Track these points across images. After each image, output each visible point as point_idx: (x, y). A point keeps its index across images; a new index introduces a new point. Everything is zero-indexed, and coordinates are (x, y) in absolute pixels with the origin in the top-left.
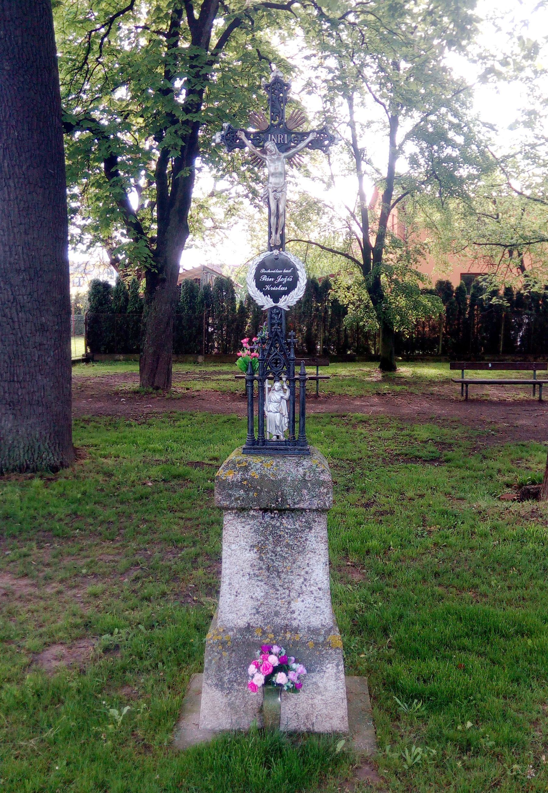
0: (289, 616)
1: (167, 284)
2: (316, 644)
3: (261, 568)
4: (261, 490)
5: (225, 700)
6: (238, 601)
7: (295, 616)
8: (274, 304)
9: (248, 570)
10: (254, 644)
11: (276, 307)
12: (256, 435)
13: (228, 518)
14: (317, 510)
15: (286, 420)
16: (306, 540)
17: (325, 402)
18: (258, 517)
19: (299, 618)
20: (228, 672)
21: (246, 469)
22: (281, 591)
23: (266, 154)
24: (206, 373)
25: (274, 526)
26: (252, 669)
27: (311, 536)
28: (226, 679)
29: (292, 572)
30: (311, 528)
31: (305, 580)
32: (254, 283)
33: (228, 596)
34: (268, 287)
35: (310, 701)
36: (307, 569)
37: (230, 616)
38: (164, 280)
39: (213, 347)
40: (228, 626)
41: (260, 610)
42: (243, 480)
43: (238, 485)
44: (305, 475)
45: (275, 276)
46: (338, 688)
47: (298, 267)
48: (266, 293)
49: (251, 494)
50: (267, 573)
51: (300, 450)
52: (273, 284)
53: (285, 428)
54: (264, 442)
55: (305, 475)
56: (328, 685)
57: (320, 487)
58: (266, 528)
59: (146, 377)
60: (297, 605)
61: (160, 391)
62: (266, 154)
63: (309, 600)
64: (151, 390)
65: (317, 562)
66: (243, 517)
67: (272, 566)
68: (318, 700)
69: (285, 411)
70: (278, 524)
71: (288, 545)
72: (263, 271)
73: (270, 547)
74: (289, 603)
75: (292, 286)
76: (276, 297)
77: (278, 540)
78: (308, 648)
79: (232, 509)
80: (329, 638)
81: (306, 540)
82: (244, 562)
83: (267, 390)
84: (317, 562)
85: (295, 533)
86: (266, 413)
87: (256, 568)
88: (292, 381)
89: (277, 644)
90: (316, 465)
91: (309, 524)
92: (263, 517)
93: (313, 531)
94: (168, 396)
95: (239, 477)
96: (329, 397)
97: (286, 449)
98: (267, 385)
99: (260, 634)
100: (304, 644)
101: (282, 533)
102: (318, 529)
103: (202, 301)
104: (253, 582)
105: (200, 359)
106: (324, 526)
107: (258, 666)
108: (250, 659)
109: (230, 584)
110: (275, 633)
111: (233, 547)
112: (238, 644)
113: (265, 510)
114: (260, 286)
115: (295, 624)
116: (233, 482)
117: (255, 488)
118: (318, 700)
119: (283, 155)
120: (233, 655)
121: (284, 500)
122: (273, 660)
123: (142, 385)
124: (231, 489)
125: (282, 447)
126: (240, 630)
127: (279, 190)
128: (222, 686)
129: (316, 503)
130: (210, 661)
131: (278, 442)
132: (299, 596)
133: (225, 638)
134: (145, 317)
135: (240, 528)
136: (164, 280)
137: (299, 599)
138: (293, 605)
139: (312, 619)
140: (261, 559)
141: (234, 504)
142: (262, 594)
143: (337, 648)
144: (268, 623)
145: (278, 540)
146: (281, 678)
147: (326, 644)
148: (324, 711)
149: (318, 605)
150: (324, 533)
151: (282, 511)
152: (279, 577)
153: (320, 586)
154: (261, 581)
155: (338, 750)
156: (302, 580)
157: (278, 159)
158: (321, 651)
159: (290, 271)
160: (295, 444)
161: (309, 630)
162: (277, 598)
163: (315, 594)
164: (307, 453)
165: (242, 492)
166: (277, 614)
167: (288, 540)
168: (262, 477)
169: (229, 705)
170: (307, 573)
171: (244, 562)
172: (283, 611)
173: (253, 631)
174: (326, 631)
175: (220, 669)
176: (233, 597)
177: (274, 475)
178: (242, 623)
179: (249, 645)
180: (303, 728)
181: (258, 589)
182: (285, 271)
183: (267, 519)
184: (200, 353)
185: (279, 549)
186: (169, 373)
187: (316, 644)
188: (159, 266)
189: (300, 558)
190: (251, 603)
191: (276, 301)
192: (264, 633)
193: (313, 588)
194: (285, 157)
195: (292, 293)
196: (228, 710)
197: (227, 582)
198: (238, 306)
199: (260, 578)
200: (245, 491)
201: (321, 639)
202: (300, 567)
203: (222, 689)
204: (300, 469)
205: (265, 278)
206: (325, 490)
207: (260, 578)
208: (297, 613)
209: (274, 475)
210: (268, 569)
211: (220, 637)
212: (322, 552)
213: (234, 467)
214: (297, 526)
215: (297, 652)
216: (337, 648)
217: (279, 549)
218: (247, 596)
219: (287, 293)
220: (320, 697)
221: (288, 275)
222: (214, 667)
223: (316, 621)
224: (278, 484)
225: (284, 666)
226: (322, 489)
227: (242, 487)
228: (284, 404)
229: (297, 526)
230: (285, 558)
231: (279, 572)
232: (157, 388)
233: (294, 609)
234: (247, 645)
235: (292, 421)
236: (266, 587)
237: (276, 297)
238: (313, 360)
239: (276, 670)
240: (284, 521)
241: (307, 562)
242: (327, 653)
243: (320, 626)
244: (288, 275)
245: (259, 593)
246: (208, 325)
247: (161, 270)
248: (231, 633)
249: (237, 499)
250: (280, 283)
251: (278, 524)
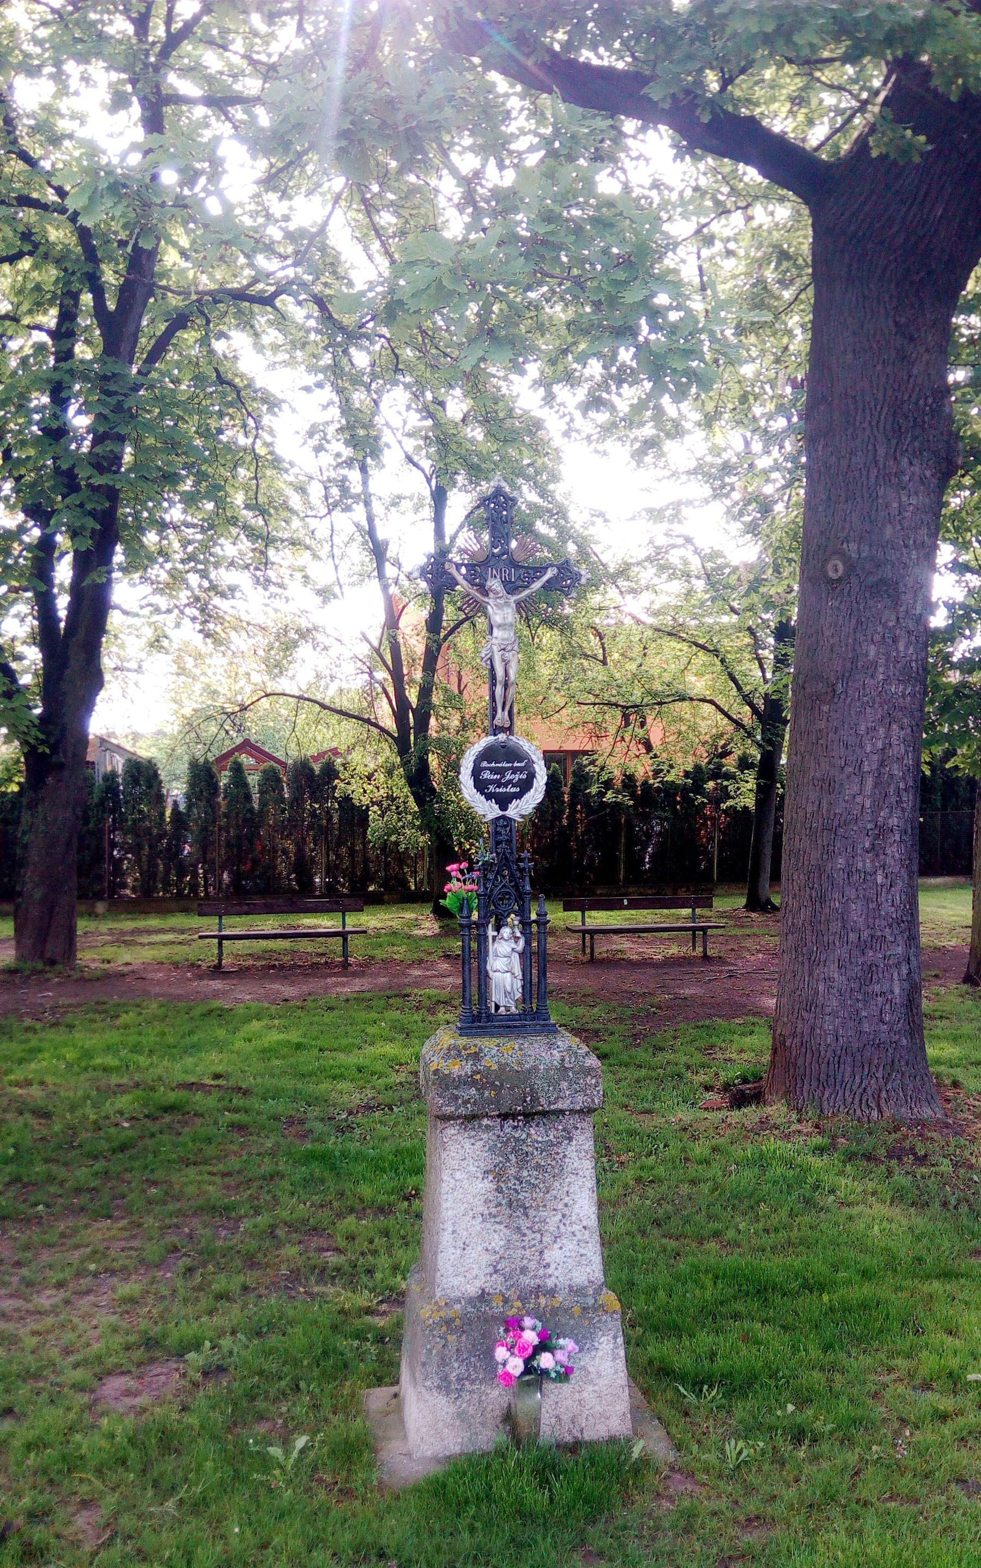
0: (541, 1272)
3: (500, 1204)
7: (550, 1271)
9: (481, 1209)
11: (503, 817)
14: (581, 1111)
15: (520, 984)
17: (362, 974)
21: (476, 1057)
24: (123, 933)
25: (517, 1140)
28: (453, 1377)
30: (570, 1139)
33: (452, 1250)
34: (492, 788)
36: (567, 1200)
37: (455, 1282)
38: (61, 767)
39: (124, 885)
43: (468, 1081)
45: (501, 771)
47: (534, 758)
48: (489, 797)
49: (487, 1094)
50: (508, 1211)
52: (499, 784)
53: (518, 995)
54: (489, 1017)
58: (506, 1144)
60: (554, 1255)
61: (59, 967)
63: (570, 1246)
64: (40, 966)
67: (515, 1199)
68: (588, 1393)
69: (518, 971)
71: (538, 1167)
72: (485, 764)
74: (541, 1253)
75: (526, 785)
76: (503, 802)
78: (572, 1317)
79: (459, 1117)
89: (528, 1314)
94: (76, 975)
95: (468, 1068)
96: (365, 967)
103: (102, 802)
107: (510, 1349)
109: (454, 1232)
111: (458, 1175)
113: (504, 1117)
115: (550, 1283)
118: (588, 1393)
121: (535, 1099)
122: (531, 1337)
125: (517, 1023)
126: (471, 1301)
129: (580, 1101)
131: (511, 1017)
133: (451, 1314)
134: (24, 833)
135: (467, 1145)
136: (61, 767)
139: (575, 1274)
141: (462, 1111)
146: (546, 1361)
147: (600, 1308)
148: (598, 1408)
149: (583, 1251)
150: (589, 1145)
151: (529, 1116)
152: (527, 1215)
160: (531, 1017)
161: (571, 1291)
163: (579, 1236)
165: (473, 1091)
166: (524, 1270)
168: (502, 1067)
172: (533, 1265)
176: (459, 1252)
178: (472, 1290)
179: (486, 1320)
185: (525, 1173)
186: (72, 931)
191: (504, 807)
192: (506, 1301)
193: (575, 1228)
201: (591, 1301)
203: (448, 1392)
205: (487, 775)
208: (553, 1266)
209: (519, 1064)
211: (442, 1314)
212: (587, 1173)
213: (459, 1055)
217: (525, 1173)
219: (519, 796)
220: (591, 1388)
221: (521, 770)
225: (544, 1345)
227: (474, 1083)
228: (516, 958)
230: (535, 1186)
233: (548, 1260)
235: (527, 984)
236: (508, 1232)
237: (503, 802)
244: (521, 770)
245: (497, 1242)
246: (113, 845)
247: (55, 748)
248: (457, 1307)
249: (466, 1102)
250: (510, 782)
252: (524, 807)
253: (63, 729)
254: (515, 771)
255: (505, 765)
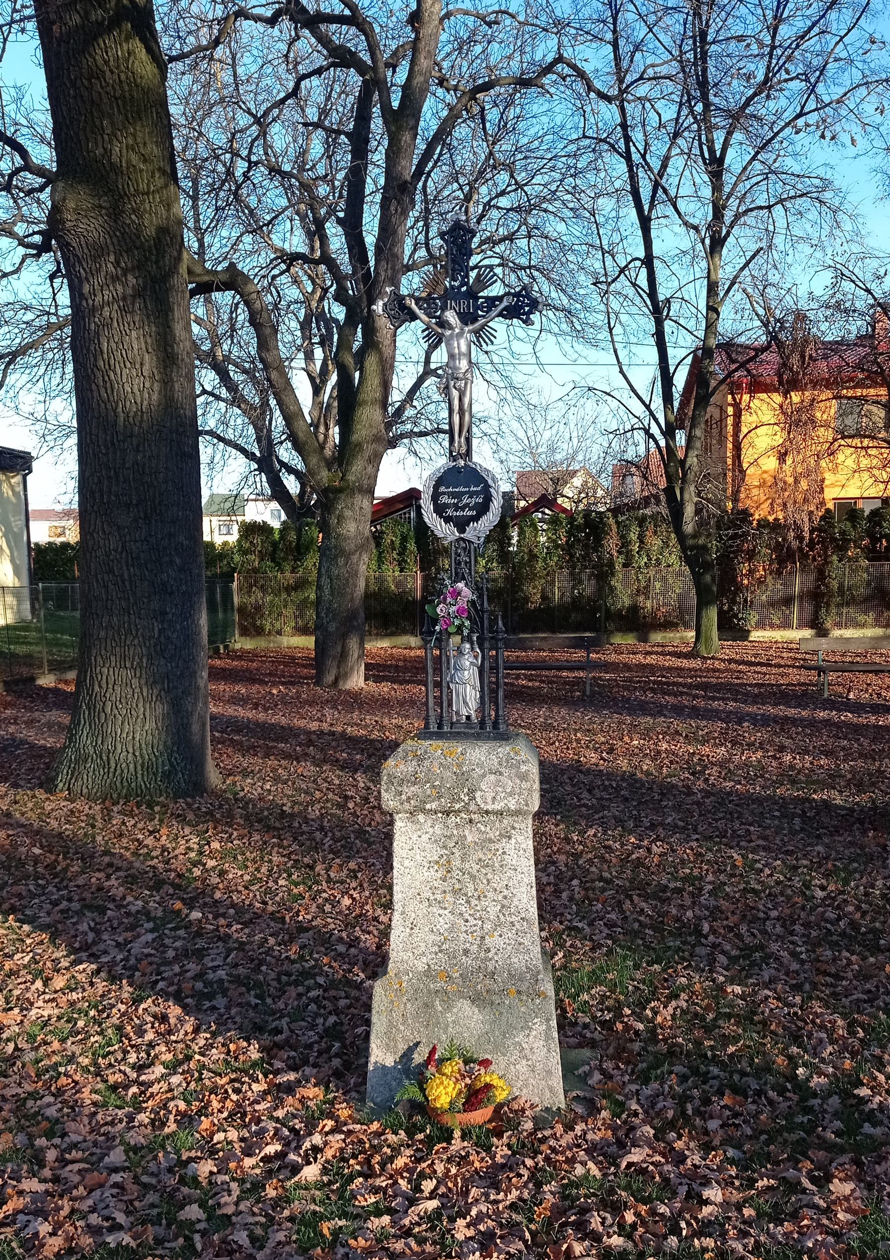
7: (490, 955)
22: (472, 922)
30: (510, 838)
31: (503, 906)
34: (450, 512)
36: (506, 892)
45: (458, 496)
48: (448, 520)
52: (457, 508)
74: (483, 938)
75: (483, 509)
76: (462, 525)
93: (513, 841)
102: (520, 839)
109: (403, 913)
138: (488, 939)
163: (518, 926)
191: (462, 530)
205: (445, 499)
208: (493, 951)
219: (476, 519)
221: (477, 493)
223: (518, 961)
237: (462, 525)
250: (467, 505)
254: (471, 495)
255: (462, 489)
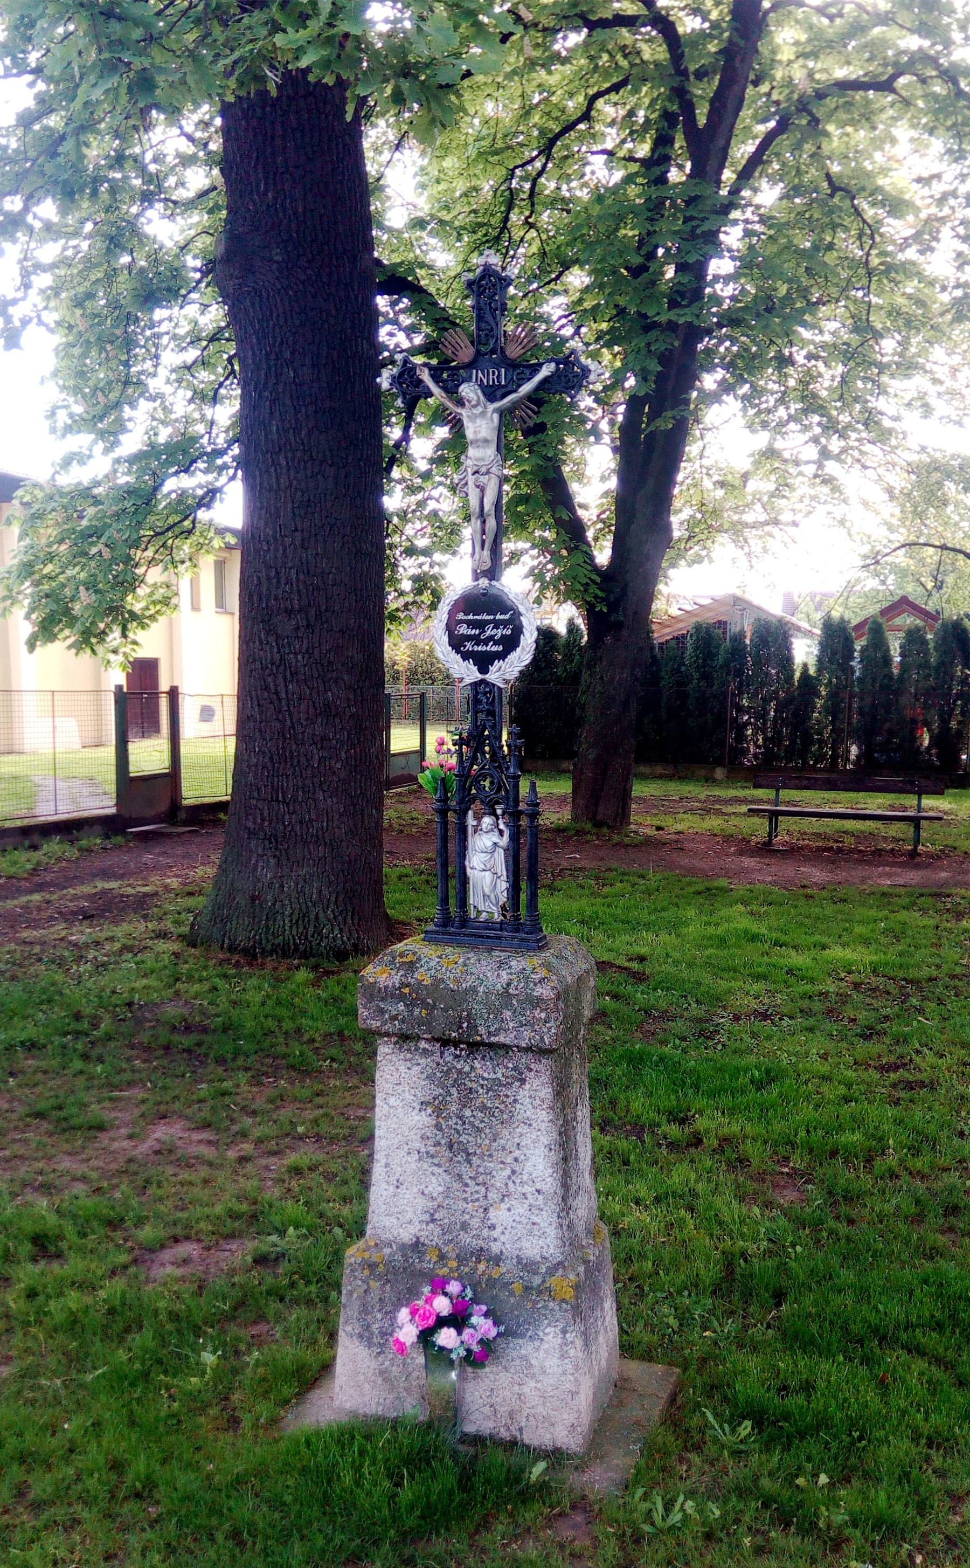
0: (485, 1232)
1: (625, 633)
2: (527, 1289)
3: (438, 1144)
4: (434, 1007)
5: (374, 1364)
6: (402, 1196)
7: (495, 1234)
8: (480, 676)
9: (417, 1145)
10: (421, 1273)
11: (483, 681)
12: (453, 909)
13: (384, 1049)
14: (528, 1049)
15: (505, 885)
16: (515, 1101)
18: (433, 1053)
19: (503, 1238)
20: (379, 1316)
21: (411, 967)
22: (473, 1187)
23: (463, 405)
25: (460, 1072)
26: (404, 1314)
27: (524, 1094)
28: (375, 1327)
29: (491, 1156)
30: (523, 1081)
31: (514, 1172)
32: (446, 639)
33: (385, 1186)
34: (469, 646)
35: (516, 1388)
36: (517, 1153)
37: (388, 1222)
39: (745, 752)
40: (383, 1237)
41: (437, 1216)
42: (403, 985)
43: (395, 994)
44: (509, 985)
45: (481, 625)
46: (564, 1373)
47: (522, 609)
48: (466, 656)
49: (417, 1011)
50: (448, 1154)
51: (522, 940)
52: (477, 640)
53: (503, 899)
54: (465, 921)
55: (509, 985)
56: (547, 1364)
57: (534, 1008)
58: (448, 1073)
59: (581, 802)
60: (499, 1215)
62: (463, 405)
63: (521, 1209)
65: (534, 1142)
66: (409, 1050)
67: (459, 1141)
68: (529, 1388)
69: (501, 869)
70: (467, 1069)
71: (483, 1108)
72: (461, 616)
73: (454, 1108)
75: (511, 643)
76: (484, 662)
77: (467, 1097)
78: (512, 1294)
79: (387, 1034)
80: (552, 1282)
81: (515, 1101)
82: (410, 1129)
83: (470, 830)
84: (534, 1142)
85: (494, 1086)
86: (469, 871)
87: (430, 1142)
88: (514, 816)
89: (460, 1278)
90: (556, 968)
91: (521, 1073)
92: (442, 1053)
93: (527, 1086)
95: (397, 979)
97: (499, 938)
98: (471, 821)
99: (435, 1259)
100: (506, 1285)
101: (474, 1085)
102: (536, 1083)
103: (726, 665)
104: (425, 1166)
105: (719, 773)
106: (545, 1078)
107: (414, 1313)
108: (407, 1296)
109: (387, 1165)
110: (461, 1259)
111: (392, 1101)
112: (395, 1271)
113: (445, 1043)
114: (456, 643)
115: (495, 1248)
116: (386, 987)
117: (424, 1001)
118: (529, 1388)
119: (491, 407)
120: (388, 1287)
121: (473, 1027)
122: (442, 1305)
123: (575, 818)
124: (383, 999)
125: (492, 933)
126: (403, 1247)
127: (483, 470)
128: (369, 1340)
129: (527, 1037)
130: (350, 1293)
131: (488, 925)
132: (502, 1200)
133: (375, 1258)
135: (403, 1069)
137: (503, 1206)
138: (492, 1213)
139: (525, 1244)
140: (438, 1127)
141: (388, 1027)
142: (441, 1189)
143: (563, 1300)
144: (451, 1241)
145: (467, 1097)
146: (446, 1337)
147: (544, 1291)
148: (541, 1409)
149: (536, 1219)
150: (546, 1092)
151: (474, 1047)
152: (469, 1162)
153: (538, 1186)
154: (439, 1165)
155: (533, 1477)
156: (508, 1172)
157: (483, 414)
158: (535, 1302)
159: (507, 617)
160: (520, 928)
161: (519, 1263)
162: (465, 1199)
163: (531, 1200)
164: (540, 945)
165: (401, 1007)
166: (465, 1226)
167: (484, 1098)
168: (437, 982)
169: (382, 1373)
170: (516, 1160)
171: (410, 1129)
172: (475, 1223)
173: (425, 1253)
174: (548, 1268)
175: (365, 1310)
176: (392, 1188)
177: (457, 981)
178: (406, 1235)
179: (413, 1274)
180: (504, 1434)
181: (434, 1179)
182: (498, 617)
183: (450, 1059)
184: (719, 762)
185: (468, 1113)
187: (527, 1289)
188: (612, 598)
189: (506, 1132)
190: (422, 1203)
191: (483, 670)
192: (442, 1257)
193: (528, 1189)
194: (495, 411)
195: (513, 656)
196: (380, 1381)
197: (383, 1162)
198: (797, 675)
199: (436, 1161)
200: (406, 1005)
201: (537, 1281)
202: (504, 1149)
203: (370, 1345)
204: (504, 974)
205: (463, 630)
206: (543, 1015)
207: (436, 1161)
208: (499, 1229)
209: (457, 981)
210: (450, 1146)
211: (367, 1255)
212: (543, 1126)
213: (392, 962)
214: (499, 1075)
215: (494, 1298)
216: (563, 1300)
217: (468, 1113)
218: (415, 1190)
219: (502, 656)
220: (532, 1384)
221: (505, 623)
222: (356, 1305)
223: (532, 1249)
224: (459, 997)
225: (458, 1320)
226: (536, 1013)
227: (402, 998)
228: (500, 855)
229: (499, 1075)
230: (479, 1130)
231: (468, 1154)
232: (599, 824)
233: (493, 1221)
234: (409, 1272)
235: (514, 889)
236: (447, 1178)
237: (484, 662)
238: (912, 783)
239: (442, 1322)
240: (477, 1064)
241: (516, 1140)
242: (545, 1307)
243: (538, 1258)
244: (505, 623)
245: (435, 1186)
246: (740, 709)
248: (387, 1251)
249: (394, 1018)
250: (491, 638)
251: (467, 1069)
252: (508, 670)
253: (624, 590)
254: (497, 624)
255: (485, 617)
